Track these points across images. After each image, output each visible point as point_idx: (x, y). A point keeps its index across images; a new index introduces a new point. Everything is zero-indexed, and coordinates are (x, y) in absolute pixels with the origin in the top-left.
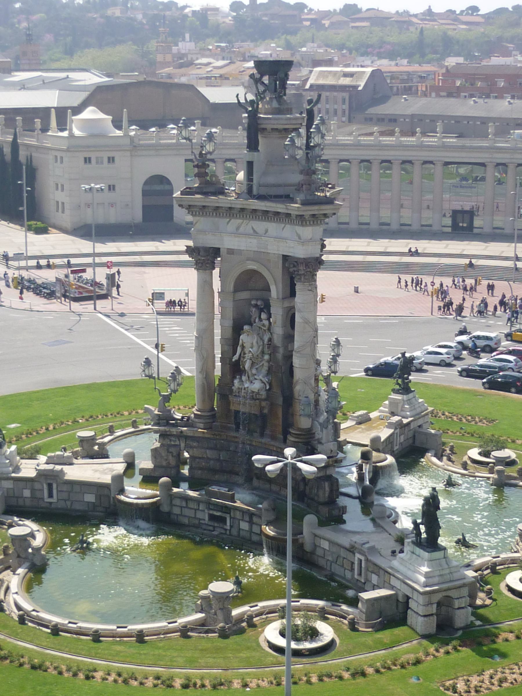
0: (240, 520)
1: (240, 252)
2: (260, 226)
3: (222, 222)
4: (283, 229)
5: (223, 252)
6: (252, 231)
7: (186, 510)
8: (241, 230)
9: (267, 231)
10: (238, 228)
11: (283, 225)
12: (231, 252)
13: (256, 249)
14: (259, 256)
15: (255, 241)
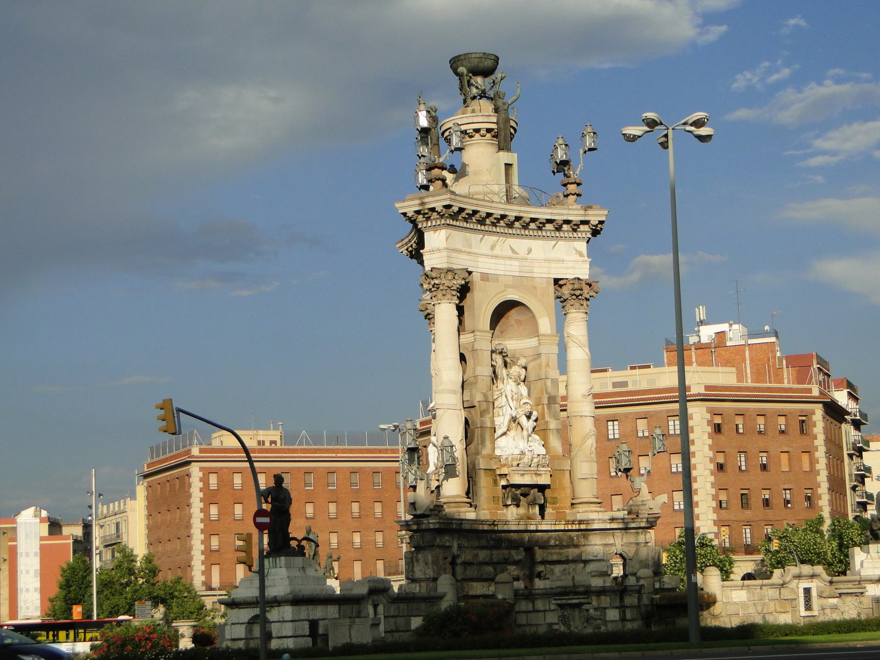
0: (605, 608)
1: (496, 278)
2: (521, 245)
3: (475, 238)
4: (554, 247)
5: (476, 277)
6: (510, 251)
7: (533, 615)
8: (497, 251)
9: (530, 251)
10: (493, 248)
11: (554, 242)
12: (485, 277)
13: (517, 274)
14: (520, 281)
15: (516, 263)
